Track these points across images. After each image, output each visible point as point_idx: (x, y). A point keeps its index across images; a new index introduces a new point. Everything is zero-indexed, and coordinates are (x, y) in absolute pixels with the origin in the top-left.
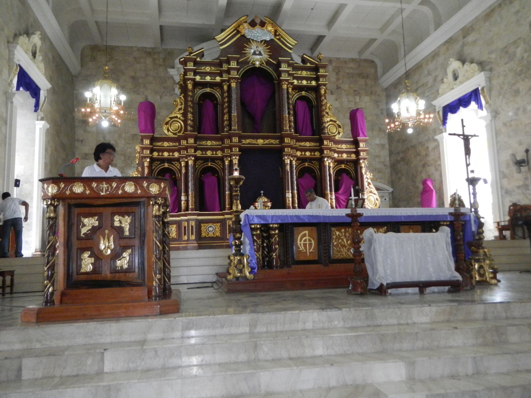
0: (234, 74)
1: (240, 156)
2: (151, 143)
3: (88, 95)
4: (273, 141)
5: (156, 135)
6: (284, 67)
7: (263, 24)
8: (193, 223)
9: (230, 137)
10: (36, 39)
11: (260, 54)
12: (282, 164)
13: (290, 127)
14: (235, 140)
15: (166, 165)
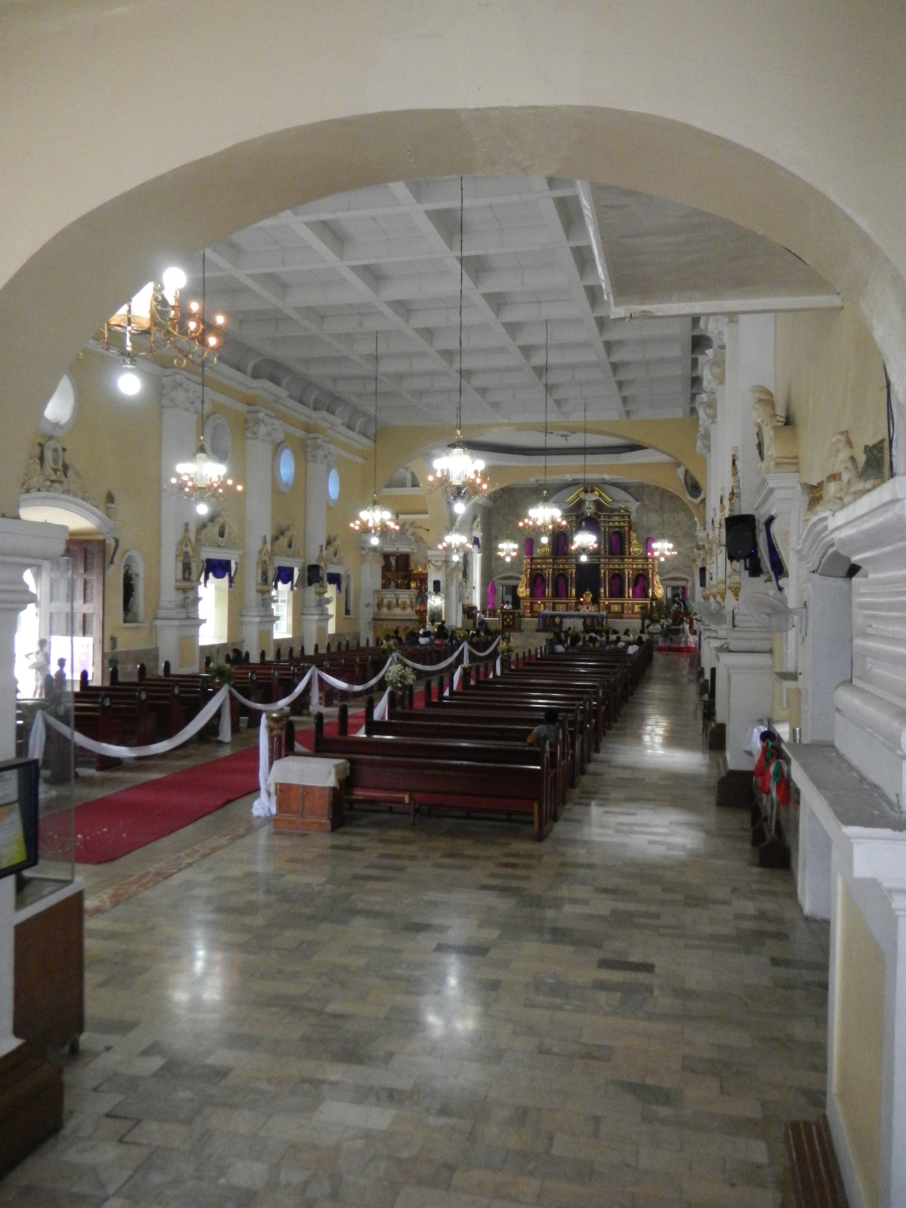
0: (574, 523)
1: (576, 569)
2: (531, 561)
3: (501, 546)
4: (595, 560)
5: (534, 556)
6: (602, 517)
7: (592, 491)
8: (551, 604)
9: (571, 558)
10: (479, 519)
11: (591, 508)
12: (599, 572)
13: (605, 551)
14: (574, 560)
15: (539, 571)
